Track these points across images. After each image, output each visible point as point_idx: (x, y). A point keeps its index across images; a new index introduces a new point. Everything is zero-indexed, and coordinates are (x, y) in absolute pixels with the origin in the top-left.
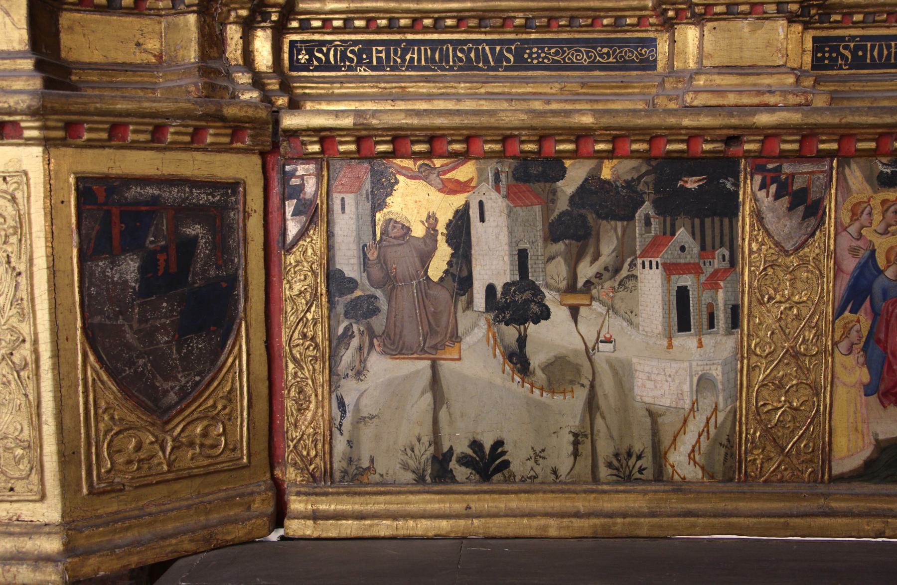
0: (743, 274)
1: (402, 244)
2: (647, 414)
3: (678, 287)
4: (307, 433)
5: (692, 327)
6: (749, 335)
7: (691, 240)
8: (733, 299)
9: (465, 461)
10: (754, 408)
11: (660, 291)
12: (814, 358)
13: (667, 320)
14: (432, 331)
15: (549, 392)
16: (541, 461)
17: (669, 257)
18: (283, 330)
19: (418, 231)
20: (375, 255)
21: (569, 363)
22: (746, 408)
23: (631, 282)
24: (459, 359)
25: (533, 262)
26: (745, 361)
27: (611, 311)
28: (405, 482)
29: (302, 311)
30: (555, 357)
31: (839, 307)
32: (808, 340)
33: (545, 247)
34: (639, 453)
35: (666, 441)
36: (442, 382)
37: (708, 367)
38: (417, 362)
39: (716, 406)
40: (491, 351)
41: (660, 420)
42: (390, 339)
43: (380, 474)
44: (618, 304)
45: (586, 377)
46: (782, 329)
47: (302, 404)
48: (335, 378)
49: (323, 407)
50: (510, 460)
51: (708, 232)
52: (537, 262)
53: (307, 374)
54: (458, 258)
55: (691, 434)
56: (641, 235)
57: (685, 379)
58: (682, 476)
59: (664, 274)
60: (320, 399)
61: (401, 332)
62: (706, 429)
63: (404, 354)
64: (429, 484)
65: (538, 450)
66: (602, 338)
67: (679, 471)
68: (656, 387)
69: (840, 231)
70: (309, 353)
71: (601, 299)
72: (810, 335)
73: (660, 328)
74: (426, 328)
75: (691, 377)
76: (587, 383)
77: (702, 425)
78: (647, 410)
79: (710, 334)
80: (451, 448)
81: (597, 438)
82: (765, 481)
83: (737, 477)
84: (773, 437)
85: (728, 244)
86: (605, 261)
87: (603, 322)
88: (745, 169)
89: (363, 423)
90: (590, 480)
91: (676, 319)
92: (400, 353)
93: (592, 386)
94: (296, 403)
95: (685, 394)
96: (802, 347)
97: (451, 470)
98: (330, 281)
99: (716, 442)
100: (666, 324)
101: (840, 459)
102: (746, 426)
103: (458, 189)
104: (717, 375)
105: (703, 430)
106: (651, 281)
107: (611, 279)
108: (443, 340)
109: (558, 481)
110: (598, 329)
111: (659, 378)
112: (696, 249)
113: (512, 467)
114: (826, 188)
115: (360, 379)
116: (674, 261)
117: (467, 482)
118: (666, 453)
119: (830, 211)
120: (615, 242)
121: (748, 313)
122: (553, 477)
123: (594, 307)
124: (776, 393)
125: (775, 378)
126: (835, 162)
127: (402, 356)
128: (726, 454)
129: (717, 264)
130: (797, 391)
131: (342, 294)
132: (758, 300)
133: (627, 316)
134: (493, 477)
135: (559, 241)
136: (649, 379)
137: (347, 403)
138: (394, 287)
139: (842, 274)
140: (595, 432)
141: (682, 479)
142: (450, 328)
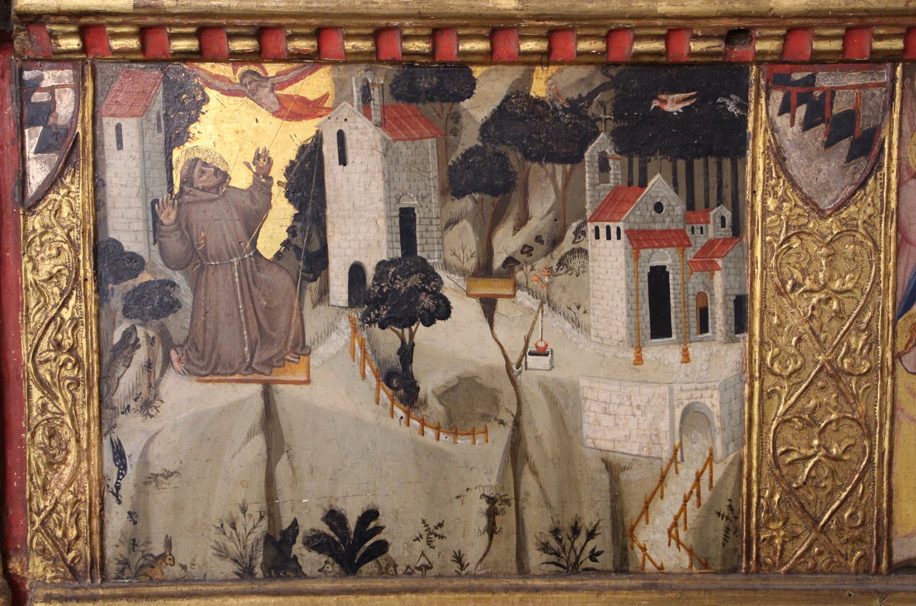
0: (752, 246)
1: (216, 200)
2: (603, 466)
3: (651, 268)
4: (64, 501)
5: (673, 330)
6: (762, 343)
7: (673, 193)
8: (737, 286)
9: (317, 542)
10: (770, 457)
11: (623, 273)
12: (864, 379)
13: (634, 320)
14: (264, 338)
15: (449, 433)
16: (437, 541)
17: (638, 220)
18: (23, 337)
19: (241, 179)
20: (173, 217)
21: (481, 387)
22: (758, 457)
23: (576, 260)
24: (308, 382)
25: (424, 228)
26: (757, 384)
27: (546, 306)
28: (221, 576)
29: (54, 307)
30: (459, 378)
31: (904, 297)
32: (855, 350)
33: (442, 205)
34: (590, 529)
35: (633, 509)
36: (280, 417)
37: (698, 394)
38: (240, 386)
39: (711, 454)
40: (357, 369)
41: (623, 477)
42: (197, 350)
44: (557, 295)
45: (507, 410)
46: (814, 333)
47: (54, 456)
48: (107, 412)
49: (89, 460)
50: (389, 540)
51: (699, 182)
52: (430, 228)
53: (63, 407)
54: (305, 221)
55: (672, 498)
56: (593, 185)
57: (663, 412)
58: (659, 564)
59: (630, 247)
60: (85, 446)
61: (215, 339)
62: (695, 491)
63: (219, 374)
66: (532, 348)
67: (653, 556)
68: (617, 425)
69: (905, 179)
70: (65, 373)
71: (530, 286)
72: (857, 342)
73: (623, 332)
74: (255, 333)
75: (672, 408)
76: (509, 419)
77: (689, 484)
78: (603, 460)
79: (701, 341)
80: (295, 523)
81: (525, 505)
82: (788, 572)
83: (744, 565)
84: (800, 503)
85: (729, 199)
86: (536, 227)
87: (534, 323)
88: (758, 81)
90: (515, 571)
91: (648, 318)
92: (213, 373)
93: (517, 424)
94: (45, 453)
95: (662, 435)
96: (845, 361)
98: (100, 260)
99: (712, 511)
100: (632, 326)
101: (905, 537)
102: (758, 486)
103: (305, 112)
104: (713, 405)
105: (691, 492)
106: (609, 258)
107: (546, 256)
108: (281, 351)
109: (464, 573)
110: (526, 333)
111: (622, 410)
112: (680, 208)
113: (391, 552)
114: (884, 110)
115: (148, 414)
116: (644, 227)
117: (319, 576)
118: (633, 529)
119: (890, 148)
120: (553, 197)
121: (761, 308)
122: (456, 566)
123: (519, 300)
124: (805, 433)
125: (803, 410)
126: (899, 69)
127: (216, 378)
128: (727, 530)
129: (712, 231)
130: (838, 430)
131: (118, 280)
132: (777, 288)
133: (571, 313)
134: (362, 568)
135: (464, 196)
136: (606, 412)
137: (127, 453)
138: (203, 268)
139: (908, 246)
140: (522, 496)
141: (658, 568)
142: (293, 333)
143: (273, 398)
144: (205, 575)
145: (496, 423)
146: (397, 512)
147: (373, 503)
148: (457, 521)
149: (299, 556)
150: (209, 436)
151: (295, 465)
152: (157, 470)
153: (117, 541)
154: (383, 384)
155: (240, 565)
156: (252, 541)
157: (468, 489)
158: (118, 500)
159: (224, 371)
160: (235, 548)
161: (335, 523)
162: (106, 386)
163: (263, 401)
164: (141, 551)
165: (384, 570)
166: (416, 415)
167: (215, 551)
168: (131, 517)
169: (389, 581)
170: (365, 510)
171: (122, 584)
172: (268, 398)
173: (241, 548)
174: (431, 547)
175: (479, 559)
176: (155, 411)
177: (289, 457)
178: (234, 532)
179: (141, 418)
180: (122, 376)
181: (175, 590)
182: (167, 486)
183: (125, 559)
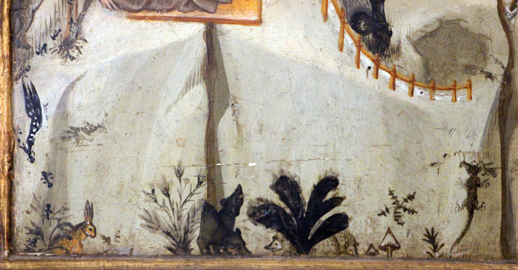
15: (424, 88)
16: (406, 217)
21: (465, 32)
24: (259, 22)
28: (151, 252)
30: (440, 21)
36: (226, 65)
38: (179, 25)
43: (104, 237)
45: (497, 61)
48: (20, 52)
50: (350, 214)
63: (154, 10)
64: (196, 256)
65: (401, 196)
76: (498, 71)
80: (239, 189)
89: (73, 140)
90: (499, 254)
92: (147, 8)
97: (238, 230)
109: (437, 255)
113: (352, 228)
117: (266, 254)
122: (428, 247)
127: (151, 14)
134: (316, 246)
137: (43, 101)
143: (217, 41)
144: (132, 249)
145: (483, 76)
146: (360, 181)
147: (331, 169)
148: (431, 193)
149: (242, 230)
150: (140, 84)
151: (241, 121)
152: (78, 124)
153: (29, 206)
154: (349, 26)
155: (174, 239)
156: (187, 211)
157: (445, 156)
158: (30, 157)
159: (160, 7)
160: (167, 218)
161: (286, 192)
162: (18, 20)
163: (205, 44)
164: (57, 219)
165: (342, 249)
166: (387, 65)
167: (144, 222)
168: (46, 178)
169: (348, 262)
170: (322, 177)
171: (34, 258)
172: (212, 40)
173: (175, 219)
174: (399, 224)
175: (455, 239)
176: (77, 51)
177: (234, 113)
178: (167, 199)
179: (60, 60)
180: (37, 8)
181: (96, 266)
182: (89, 143)
183: (37, 228)
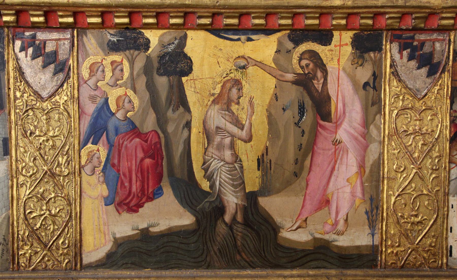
0: (10, 114)
6: (17, 160)
8: (3, 133)
10: (22, 216)
12: (66, 178)
22: (17, 215)
26: (15, 180)
31: (83, 139)
32: (62, 164)
46: (42, 156)
69: (81, 84)
72: (62, 160)
82: (33, 270)
83: (11, 267)
84: (38, 237)
88: (8, 36)
96: (57, 169)
101: (89, 252)
114: (70, 51)
119: (73, 69)
121: (16, 144)
124: (39, 204)
125: (38, 193)
126: (75, 32)
128: (3, 250)
130: (55, 202)
132: (23, 135)
139: (84, 115)
